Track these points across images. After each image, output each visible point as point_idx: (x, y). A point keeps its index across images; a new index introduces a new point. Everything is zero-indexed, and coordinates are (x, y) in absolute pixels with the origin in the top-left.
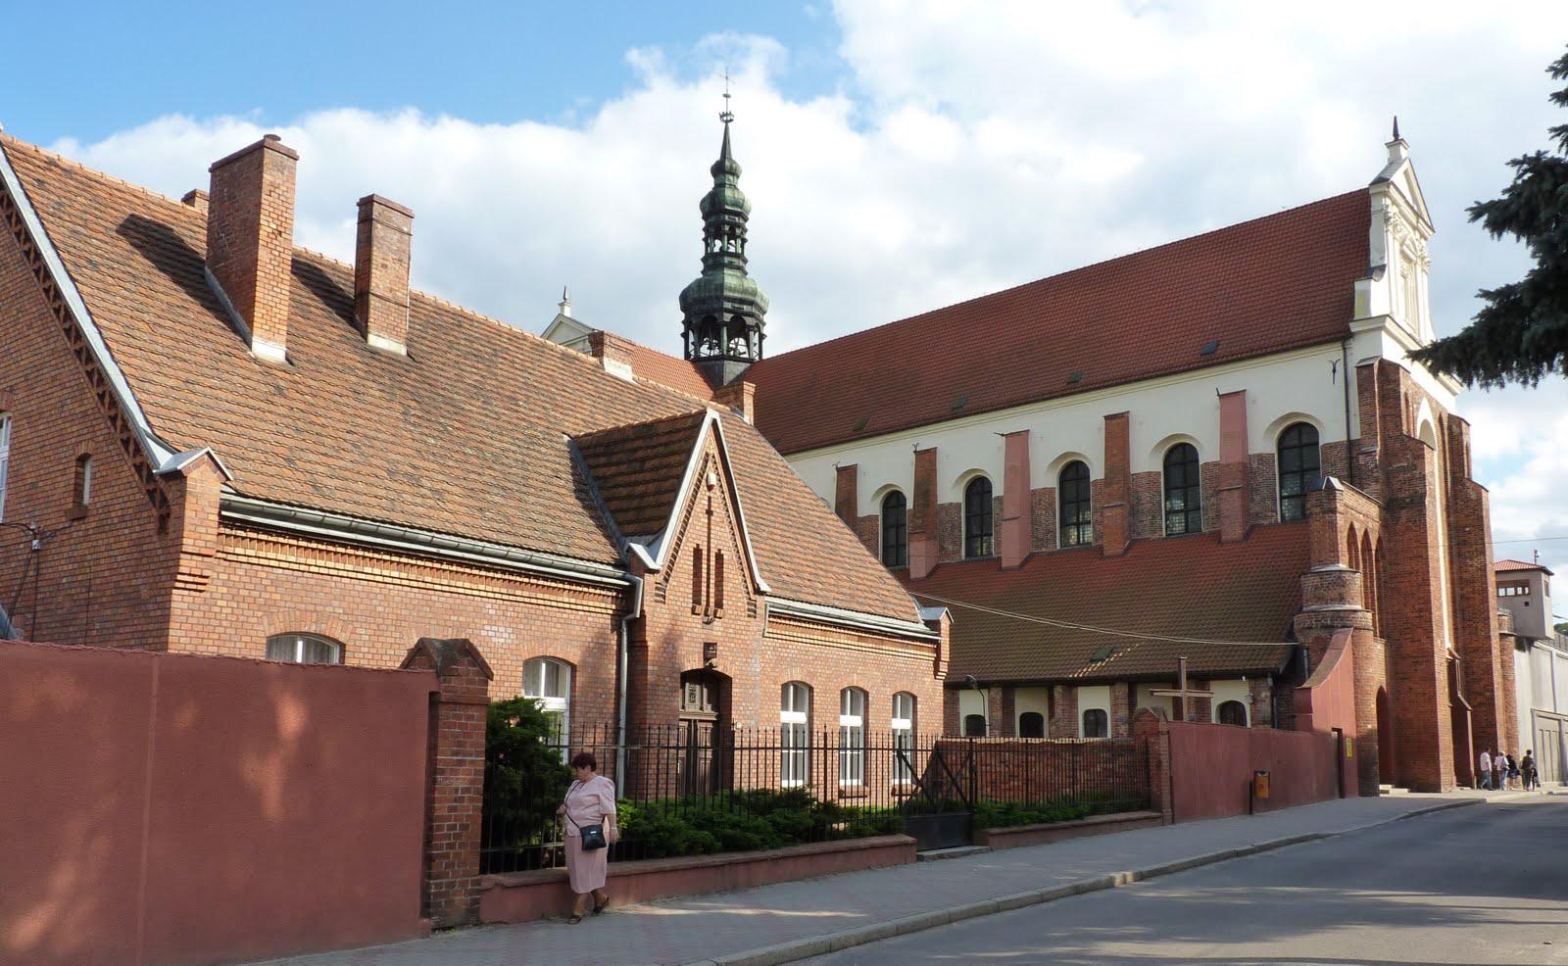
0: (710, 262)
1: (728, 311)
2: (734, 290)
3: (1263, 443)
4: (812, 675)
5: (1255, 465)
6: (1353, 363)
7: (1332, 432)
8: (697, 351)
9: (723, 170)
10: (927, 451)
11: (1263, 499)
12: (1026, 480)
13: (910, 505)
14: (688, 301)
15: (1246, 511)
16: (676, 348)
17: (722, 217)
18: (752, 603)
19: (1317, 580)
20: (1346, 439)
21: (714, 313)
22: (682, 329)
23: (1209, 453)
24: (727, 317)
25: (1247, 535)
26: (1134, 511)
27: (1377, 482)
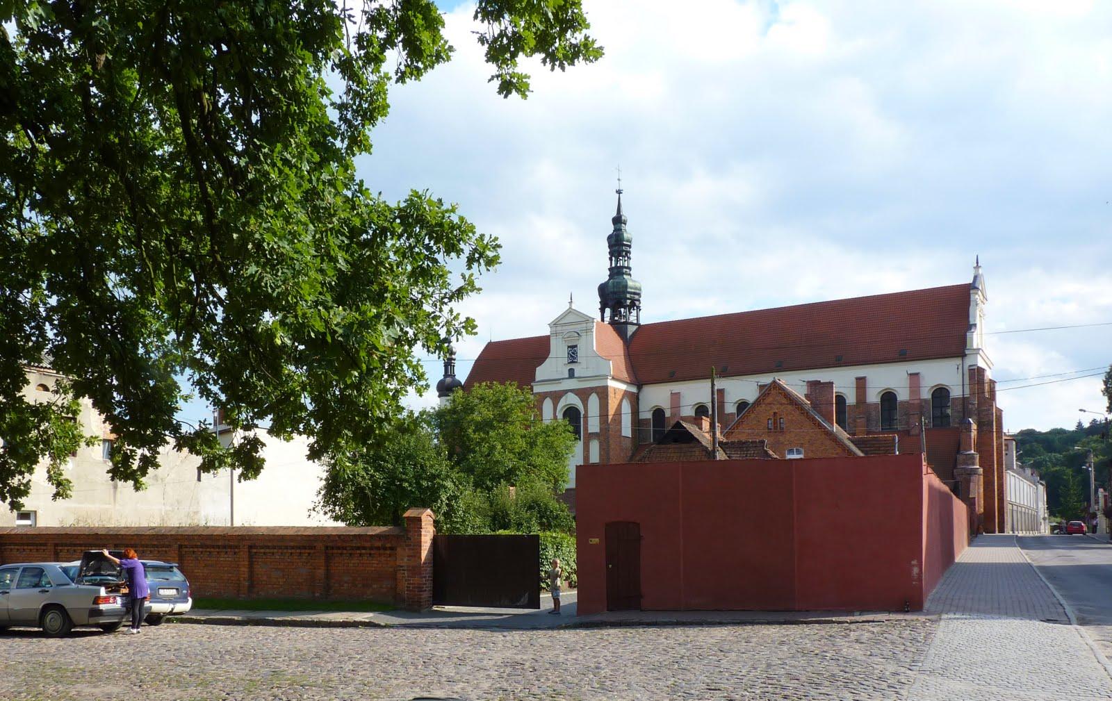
0: (616, 271)
1: (629, 299)
3: (926, 394)
7: (956, 392)
9: (618, 220)
14: (603, 289)
17: (618, 246)
23: (903, 395)
26: (868, 420)
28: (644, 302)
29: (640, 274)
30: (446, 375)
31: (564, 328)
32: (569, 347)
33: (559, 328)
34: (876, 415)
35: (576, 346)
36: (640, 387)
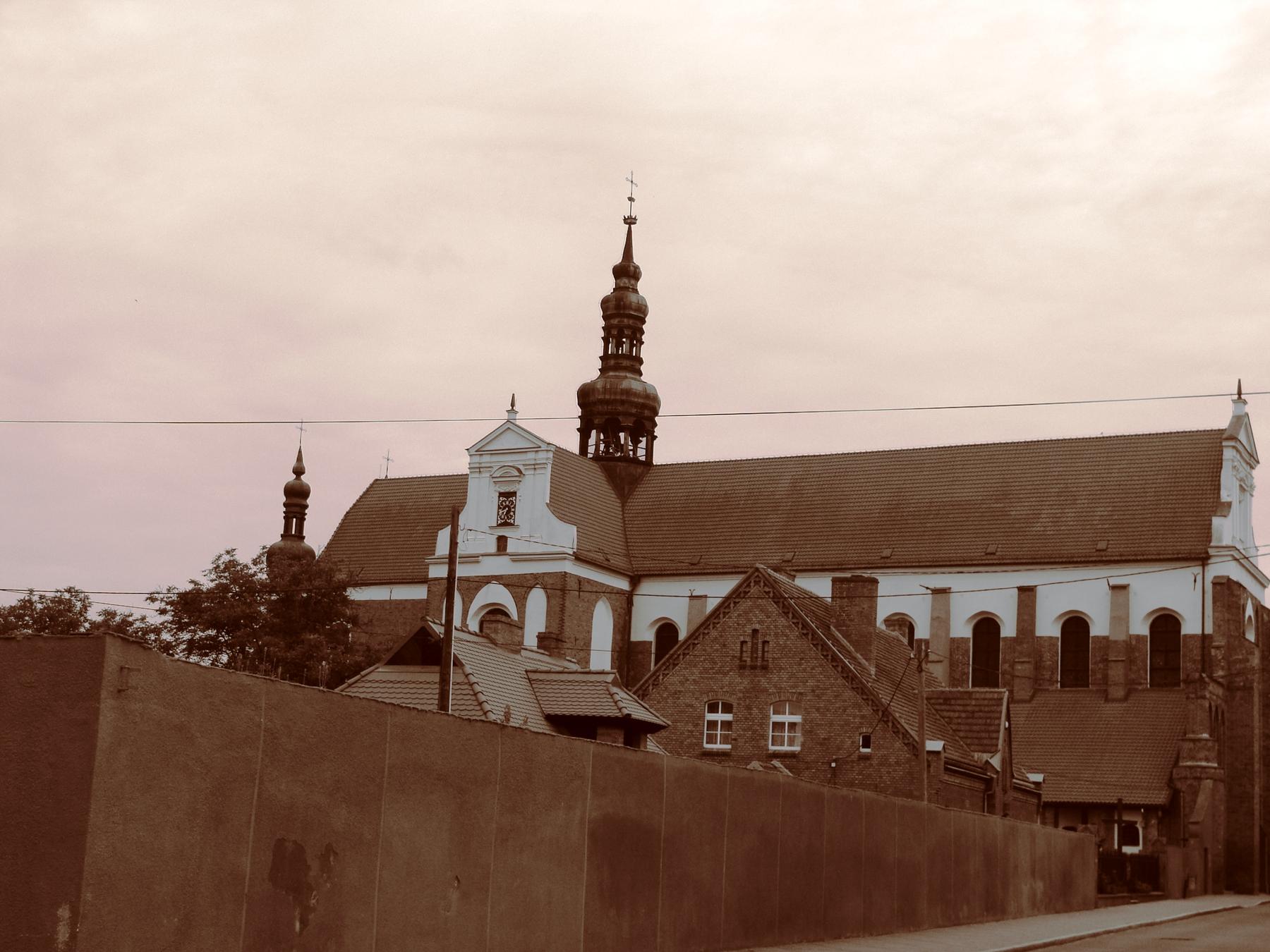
0: (612, 362)
1: (631, 415)
3: (1140, 627)
7: (1191, 626)
9: (626, 272)
12: (948, 630)
14: (585, 395)
15: (1126, 675)
16: (573, 445)
17: (623, 319)
19: (1191, 745)
20: (1200, 632)
21: (617, 412)
23: (1099, 628)
25: (1126, 698)
26: (1038, 667)
27: (1223, 668)
30: (286, 535)
31: (495, 458)
32: (501, 494)
33: (486, 459)
34: (1054, 659)
35: (514, 494)
36: (635, 581)
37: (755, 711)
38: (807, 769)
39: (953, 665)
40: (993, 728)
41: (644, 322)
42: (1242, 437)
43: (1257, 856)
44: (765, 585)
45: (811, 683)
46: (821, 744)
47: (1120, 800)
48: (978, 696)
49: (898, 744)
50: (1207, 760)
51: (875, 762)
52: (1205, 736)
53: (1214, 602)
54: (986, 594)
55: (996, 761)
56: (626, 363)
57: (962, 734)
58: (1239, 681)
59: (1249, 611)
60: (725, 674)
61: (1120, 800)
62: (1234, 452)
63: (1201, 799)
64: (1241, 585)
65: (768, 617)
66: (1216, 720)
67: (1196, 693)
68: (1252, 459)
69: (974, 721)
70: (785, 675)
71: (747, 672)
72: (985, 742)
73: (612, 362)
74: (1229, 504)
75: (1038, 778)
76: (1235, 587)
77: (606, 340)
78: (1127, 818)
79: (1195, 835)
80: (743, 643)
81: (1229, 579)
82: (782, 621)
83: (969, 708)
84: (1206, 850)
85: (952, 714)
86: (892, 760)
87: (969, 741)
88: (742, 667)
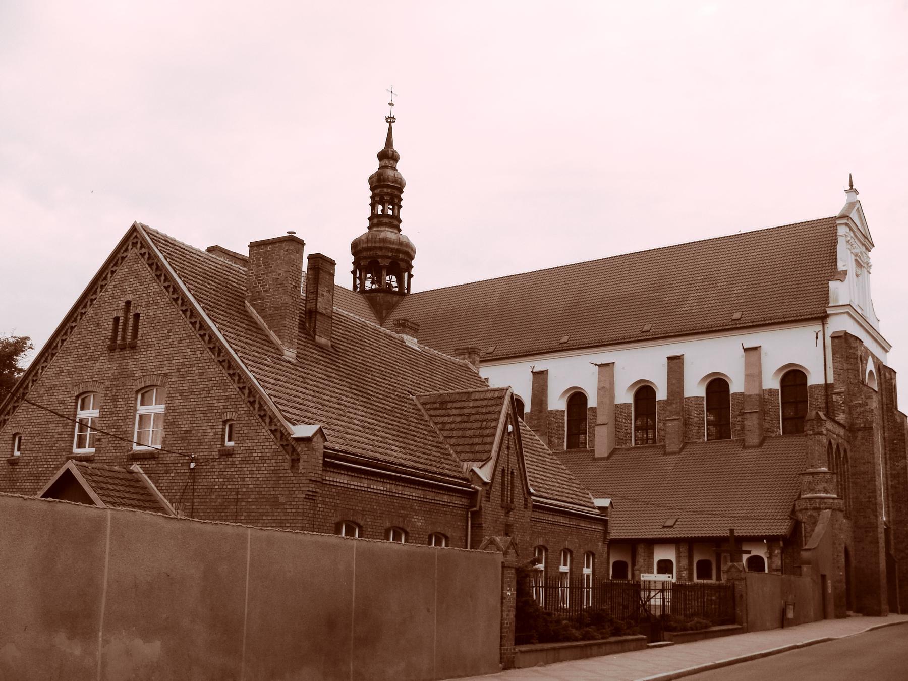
0: (375, 221)
1: (388, 257)
2: (393, 243)
3: (772, 383)
4: (547, 541)
5: (766, 396)
6: (829, 333)
7: (815, 378)
8: (362, 284)
9: (388, 156)
10: (542, 373)
11: (772, 420)
12: (612, 397)
13: (527, 409)
15: (761, 426)
17: (386, 190)
18: (526, 500)
19: (810, 478)
20: (823, 382)
22: (352, 268)
23: (737, 386)
24: (386, 263)
25: (761, 445)
26: (686, 423)
27: (844, 412)
28: (418, 264)
29: (413, 224)
37: (121, 402)
38: (167, 472)
39: (617, 427)
40: (488, 432)
41: (402, 192)
42: (854, 215)
43: (884, 581)
44: (141, 248)
45: (177, 360)
46: (182, 439)
47: (732, 531)
48: (477, 396)
49: (265, 432)
50: (826, 491)
51: (237, 458)
52: (824, 469)
53: (833, 354)
54: (642, 364)
55: (485, 473)
56: (385, 220)
57: (453, 441)
58: (860, 423)
59: (870, 366)
60: (97, 360)
61: (732, 531)
62: (848, 230)
63: (819, 528)
64: (857, 338)
65: (142, 284)
66: (836, 457)
67: (813, 430)
68: (867, 243)
69: (468, 425)
70: (152, 353)
71: (116, 354)
72: (477, 448)
73: (375, 221)
74: (845, 273)
75: (605, 502)
76: (852, 340)
77: (373, 206)
78: (760, 552)
79: (808, 563)
80: (117, 319)
81: (846, 333)
82: (155, 287)
83: (466, 411)
84: (823, 577)
85: (446, 419)
86: (256, 455)
87: (459, 449)
88: (112, 349)
